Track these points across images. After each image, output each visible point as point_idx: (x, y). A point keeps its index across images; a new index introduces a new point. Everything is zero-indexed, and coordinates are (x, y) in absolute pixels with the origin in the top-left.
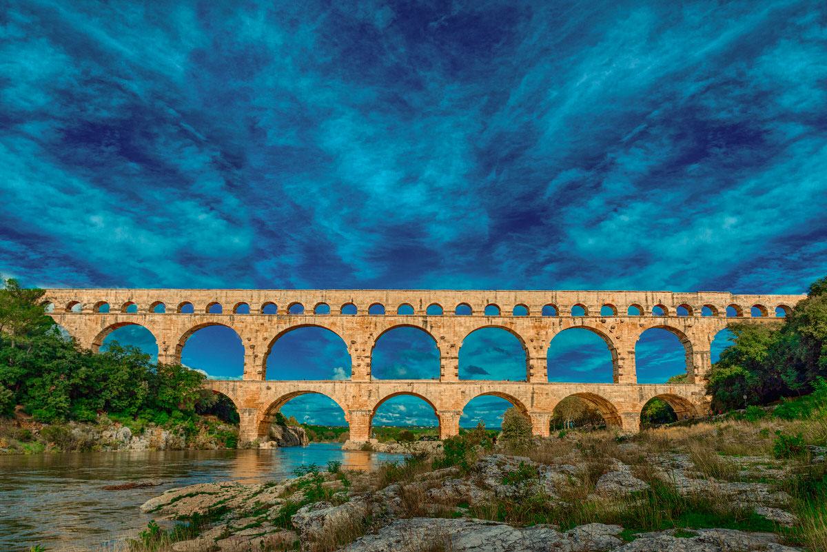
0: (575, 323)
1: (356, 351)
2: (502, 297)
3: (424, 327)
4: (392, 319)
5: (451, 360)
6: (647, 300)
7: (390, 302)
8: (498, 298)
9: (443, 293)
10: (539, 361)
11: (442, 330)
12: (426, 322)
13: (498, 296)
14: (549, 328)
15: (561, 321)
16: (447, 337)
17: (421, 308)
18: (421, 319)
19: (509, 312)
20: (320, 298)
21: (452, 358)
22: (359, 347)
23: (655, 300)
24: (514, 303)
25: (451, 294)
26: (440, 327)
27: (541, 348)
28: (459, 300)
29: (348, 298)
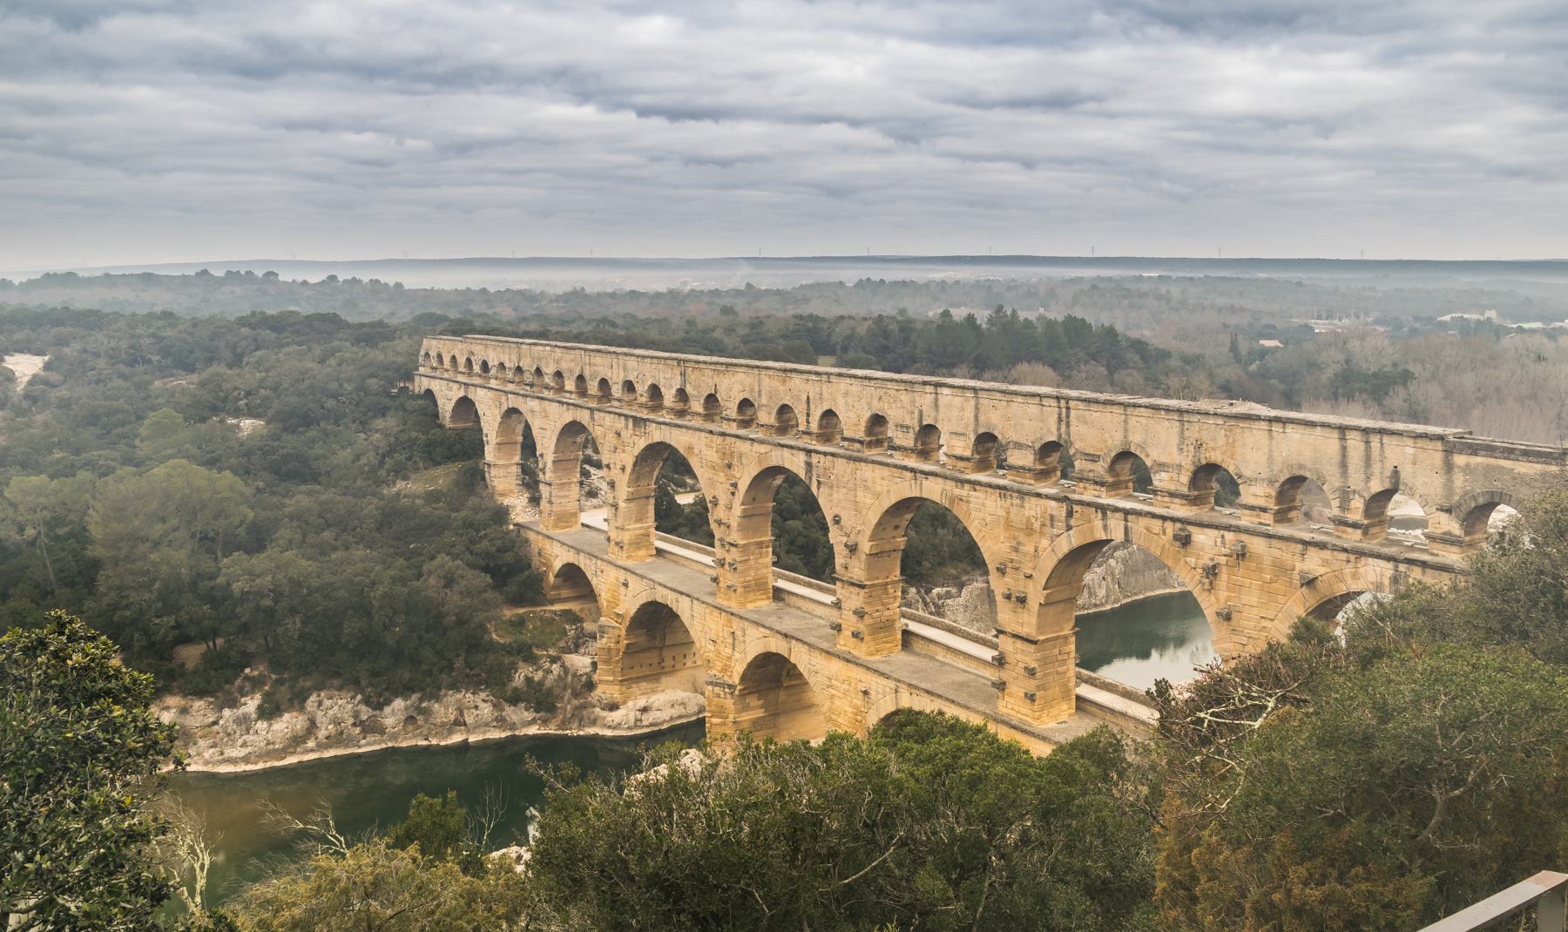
0: (1105, 527)
2: (949, 406)
4: (763, 449)
5: (852, 589)
6: (1343, 465)
7: (764, 400)
8: (942, 409)
10: (1019, 644)
12: (809, 465)
13: (942, 401)
14: (1041, 533)
15: (1070, 514)
18: (802, 457)
19: (961, 459)
21: (853, 584)
23: (1376, 468)
24: (975, 431)
27: (1022, 601)
28: (869, 404)
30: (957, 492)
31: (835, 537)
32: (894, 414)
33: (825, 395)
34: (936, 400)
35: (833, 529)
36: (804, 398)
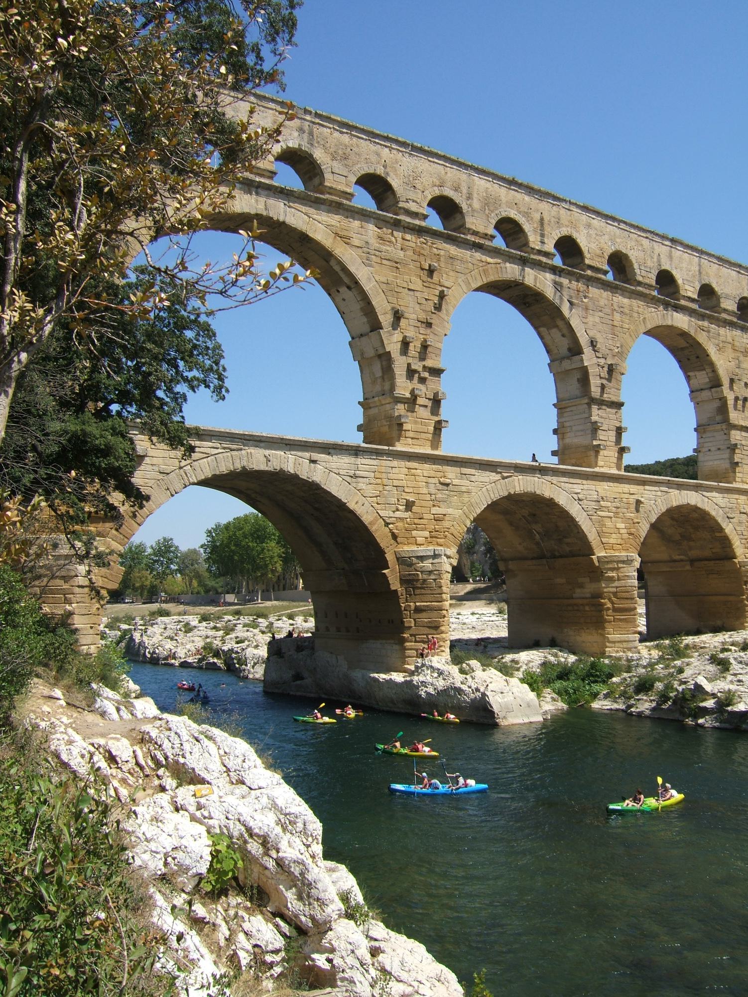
1: (405, 344)
3: (557, 301)
9: (584, 217)
11: (590, 319)
12: (558, 286)
16: (600, 338)
17: (543, 242)
18: (549, 276)
20: (296, 134)
22: (410, 333)
25: (597, 222)
26: (587, 309)
28: (613, 240)
29: (374, 158)
30: (700, 323)
31: (588, 358)
32: (634, 255)
33: (564, 221)
34: (671, 252)
35: (587, 351)
36: (537, 216)
